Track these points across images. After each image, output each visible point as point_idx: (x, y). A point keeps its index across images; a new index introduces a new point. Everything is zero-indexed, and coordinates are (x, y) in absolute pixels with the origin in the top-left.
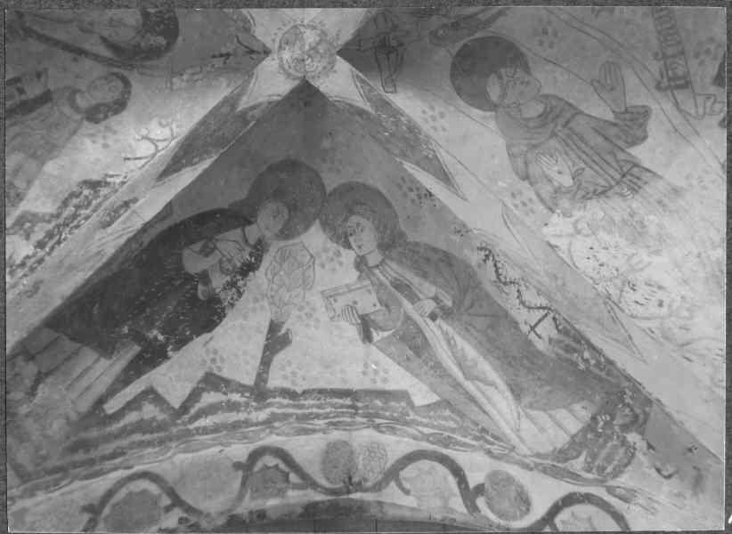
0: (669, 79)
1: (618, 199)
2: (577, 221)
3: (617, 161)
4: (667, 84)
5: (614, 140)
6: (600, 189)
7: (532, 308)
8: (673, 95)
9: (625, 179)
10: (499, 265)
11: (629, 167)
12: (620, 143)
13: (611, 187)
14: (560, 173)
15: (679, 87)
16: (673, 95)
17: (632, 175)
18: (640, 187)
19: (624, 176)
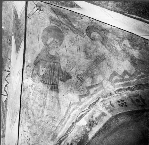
0: (81, 77)
1: (46, 87)
2: (34, 84)
3: (55, 80)
4: (79, 78)
5: (59, 76)
6: (45, 82)
7: (5, 91)
8: (78, 80)
9: (52, 86)
10: (9, 76)
11: (55, 84)
12: (59, 78)
13: (48, 84)
14: (43, 71)
15: (80, 80)
16: (78, 80)
17: (54, 86)
18: (53, 90)
19: (52, 84)
